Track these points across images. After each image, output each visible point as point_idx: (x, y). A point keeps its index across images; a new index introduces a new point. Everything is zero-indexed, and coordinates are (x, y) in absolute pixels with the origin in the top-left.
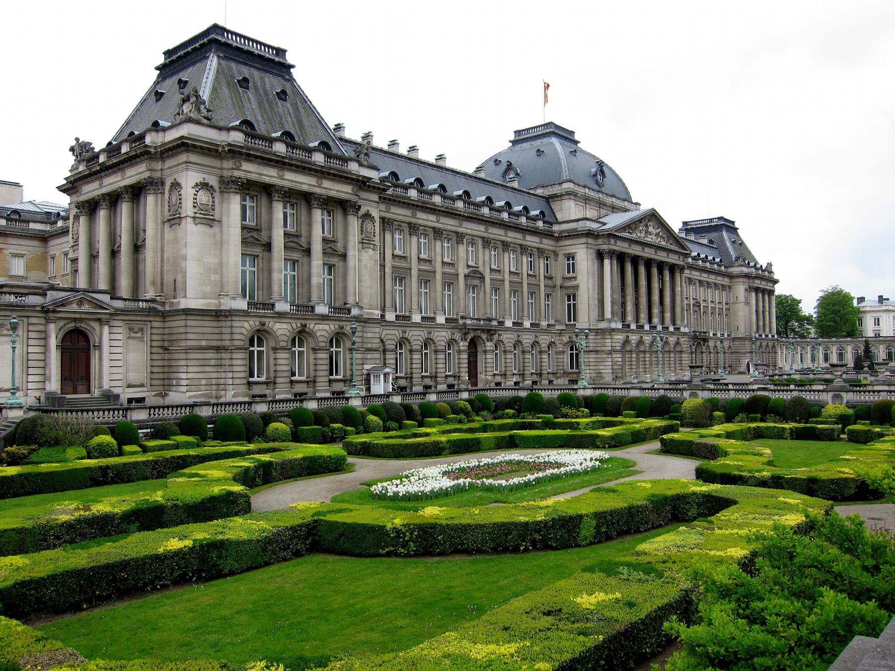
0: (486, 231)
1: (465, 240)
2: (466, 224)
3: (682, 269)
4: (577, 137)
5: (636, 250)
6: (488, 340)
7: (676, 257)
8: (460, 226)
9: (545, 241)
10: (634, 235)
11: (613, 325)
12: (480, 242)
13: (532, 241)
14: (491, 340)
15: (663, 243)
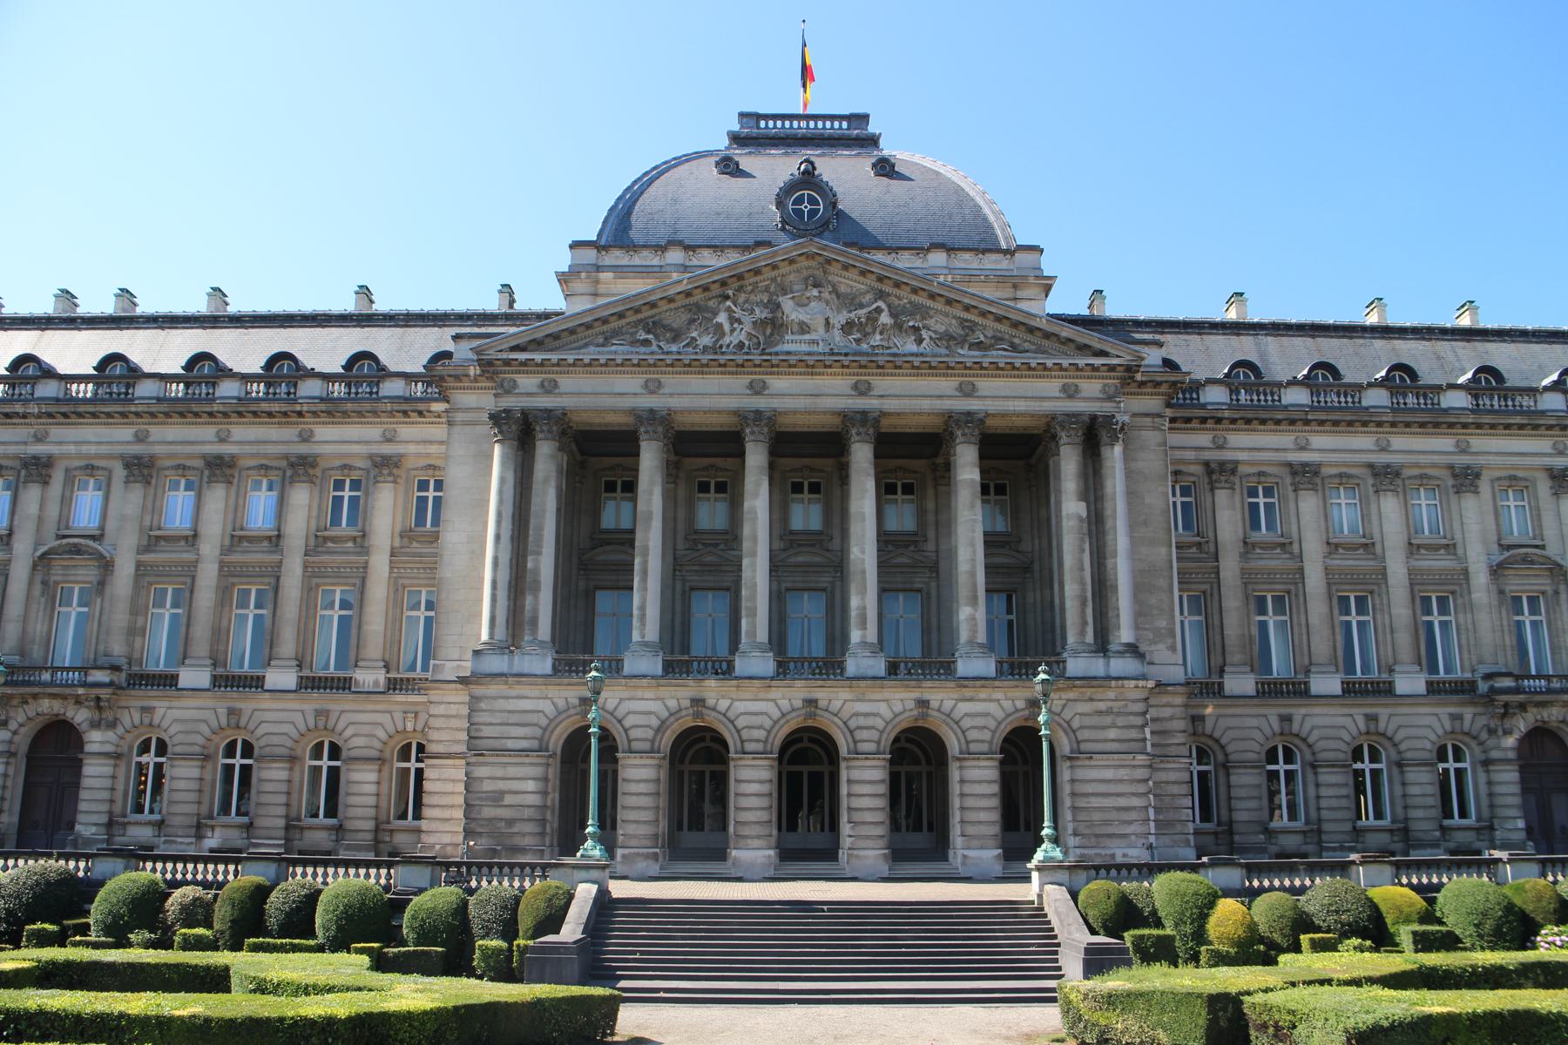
0: (140, 438)
1: (58, 476)
2: (56, 432)
3: (1094, 435)
4: (873, 128)
5: (706, 396)
6: (95, 725)
7: (1051, 386)
8: (39, 439)
9: (405, 431)
10: (674, 348)
11: (496, 663)
12: (119, 472)
13: (339, 440)
14: (112, 725)
15: (911, 347)
